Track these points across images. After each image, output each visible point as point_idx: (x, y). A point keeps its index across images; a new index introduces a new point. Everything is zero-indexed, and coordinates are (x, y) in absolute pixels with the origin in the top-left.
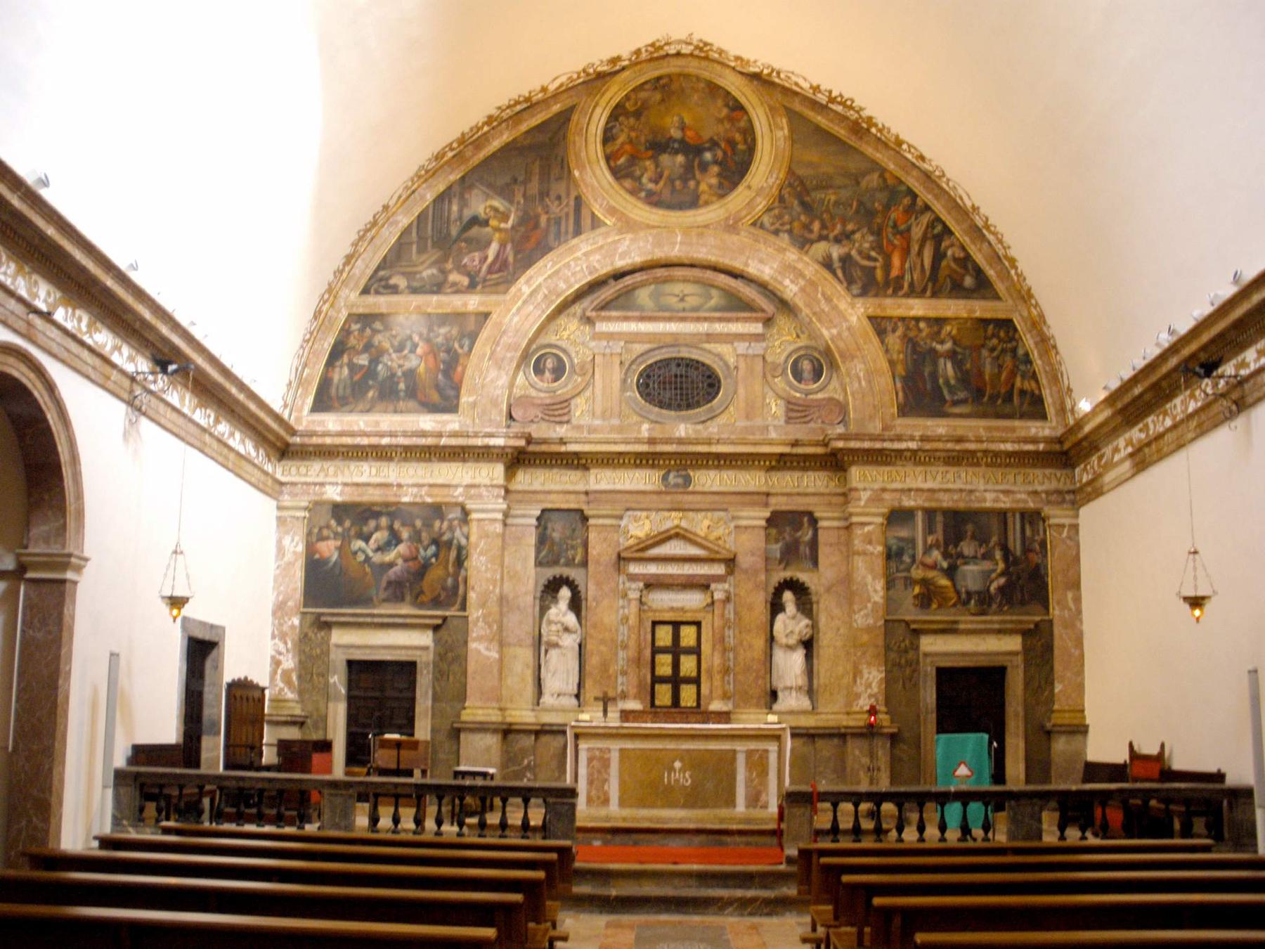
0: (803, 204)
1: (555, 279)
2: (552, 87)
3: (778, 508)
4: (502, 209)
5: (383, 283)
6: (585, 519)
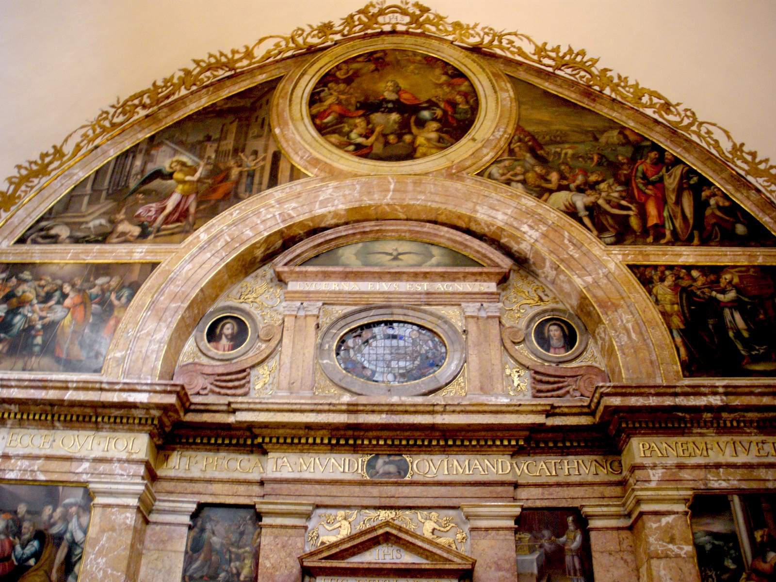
0: (536, 156)
1: (240, 226)
2: (259, 53)
3: (530, 504)
4: (190, 163)
5: (43, 233)
6: (258, 516)
